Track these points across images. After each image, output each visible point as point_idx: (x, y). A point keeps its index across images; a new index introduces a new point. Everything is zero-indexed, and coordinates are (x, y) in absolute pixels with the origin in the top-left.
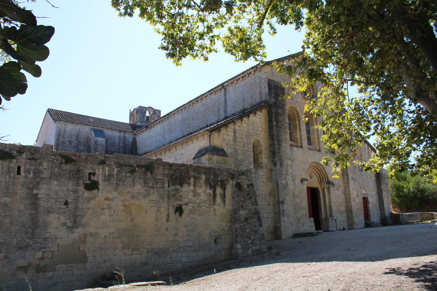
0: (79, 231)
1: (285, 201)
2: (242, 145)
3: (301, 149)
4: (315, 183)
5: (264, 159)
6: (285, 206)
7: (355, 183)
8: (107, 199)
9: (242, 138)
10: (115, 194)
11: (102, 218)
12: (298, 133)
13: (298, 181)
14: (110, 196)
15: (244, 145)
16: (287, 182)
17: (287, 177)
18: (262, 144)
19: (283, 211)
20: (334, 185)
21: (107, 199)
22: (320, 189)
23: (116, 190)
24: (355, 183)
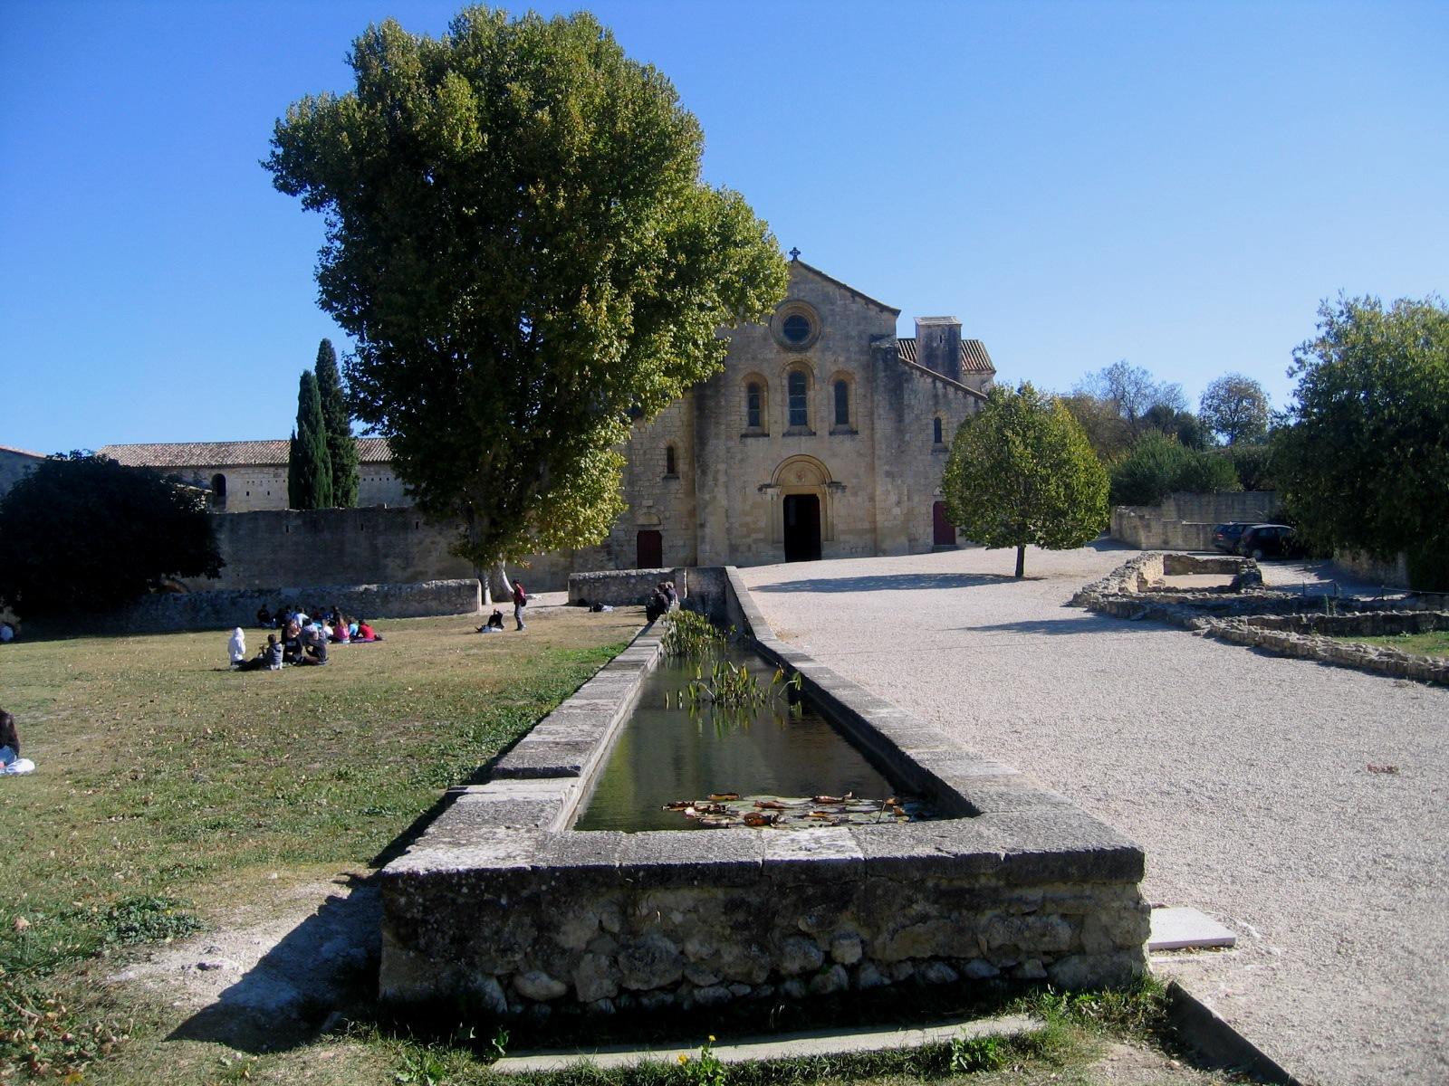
0: (410, 570)
1: (708, 525)
2: (641, 452)
3: (766, 439)
4: (807, 486)
5: (682, 466)
6: (708, 530)
7: (894, 480)
8: (433, 543)
9: (642, 444)
10: (439, 538)
11: (431, 558)
12: (766, 413)
13: (752, 489)
14: (435, 540)
15: (645, 452)
16: (715, 497)
17: (716, 489)
18: (680, 444)
19: (703, 537)
20: (844, 488)
21: (433, 543)
22: (820, 496)
23: (440, 534)
24: (894, 480)
